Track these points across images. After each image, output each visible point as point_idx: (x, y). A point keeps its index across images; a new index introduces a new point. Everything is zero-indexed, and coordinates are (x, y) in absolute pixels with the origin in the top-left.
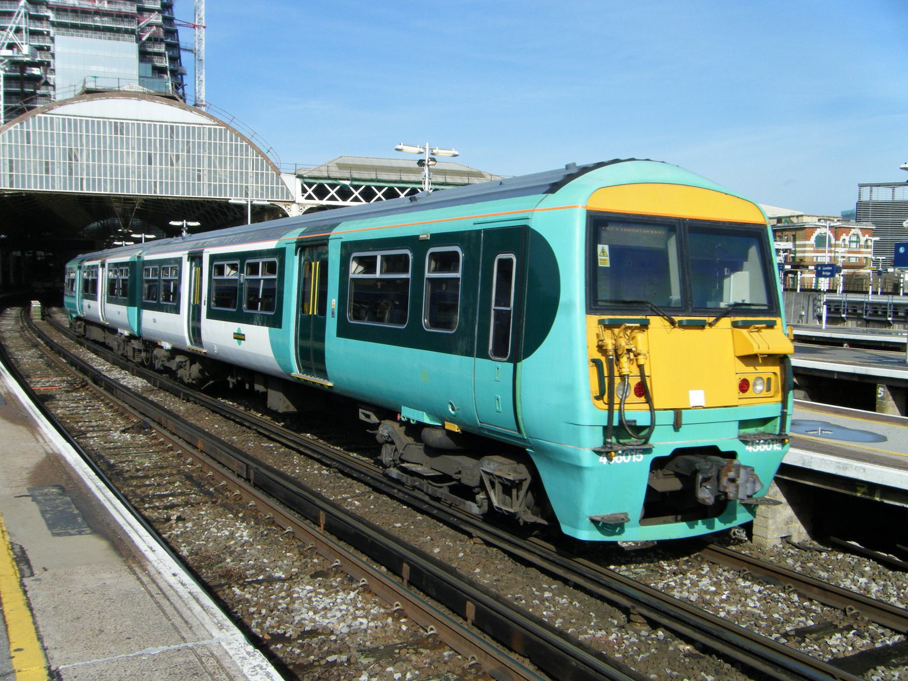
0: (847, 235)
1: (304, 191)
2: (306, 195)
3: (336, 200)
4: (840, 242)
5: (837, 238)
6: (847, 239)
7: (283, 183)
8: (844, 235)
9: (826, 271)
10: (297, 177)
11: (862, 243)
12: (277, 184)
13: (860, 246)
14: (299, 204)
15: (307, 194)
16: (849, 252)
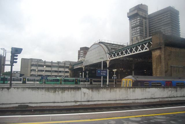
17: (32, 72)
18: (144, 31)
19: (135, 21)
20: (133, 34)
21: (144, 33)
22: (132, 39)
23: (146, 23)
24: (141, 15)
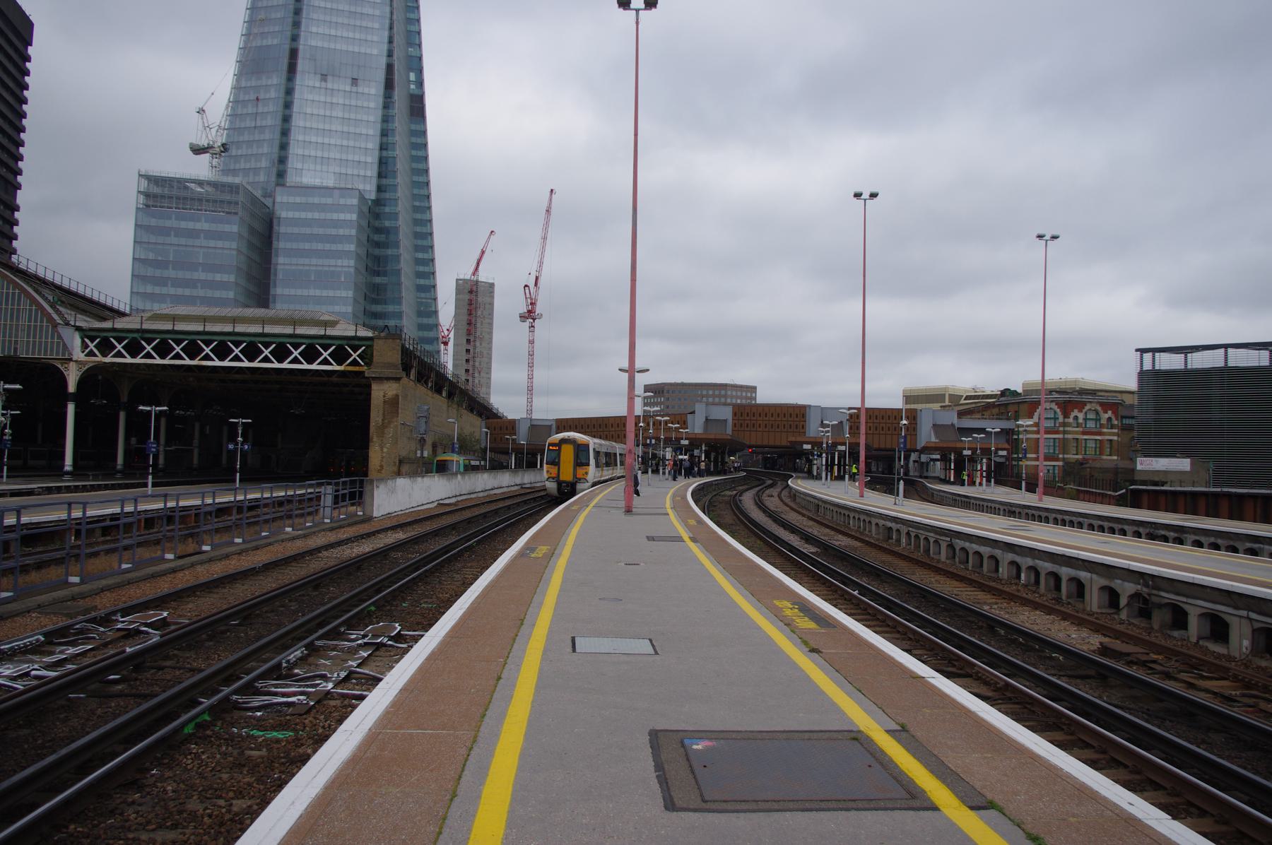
0: (1080, 411)
1: (85, 346)
2: (87, 351)
3: (124, 357)
4: (1071, 420)
5: (1066, 415)
6: (1081, 416)
7: (60, 337)
8: (1076, 411)
10: (76, 330)
11: (1104, 421)
12: (53, 338)
13: (1102, 426)
14: (76, 361)
15: (89, 349)
16: (1084, 433)
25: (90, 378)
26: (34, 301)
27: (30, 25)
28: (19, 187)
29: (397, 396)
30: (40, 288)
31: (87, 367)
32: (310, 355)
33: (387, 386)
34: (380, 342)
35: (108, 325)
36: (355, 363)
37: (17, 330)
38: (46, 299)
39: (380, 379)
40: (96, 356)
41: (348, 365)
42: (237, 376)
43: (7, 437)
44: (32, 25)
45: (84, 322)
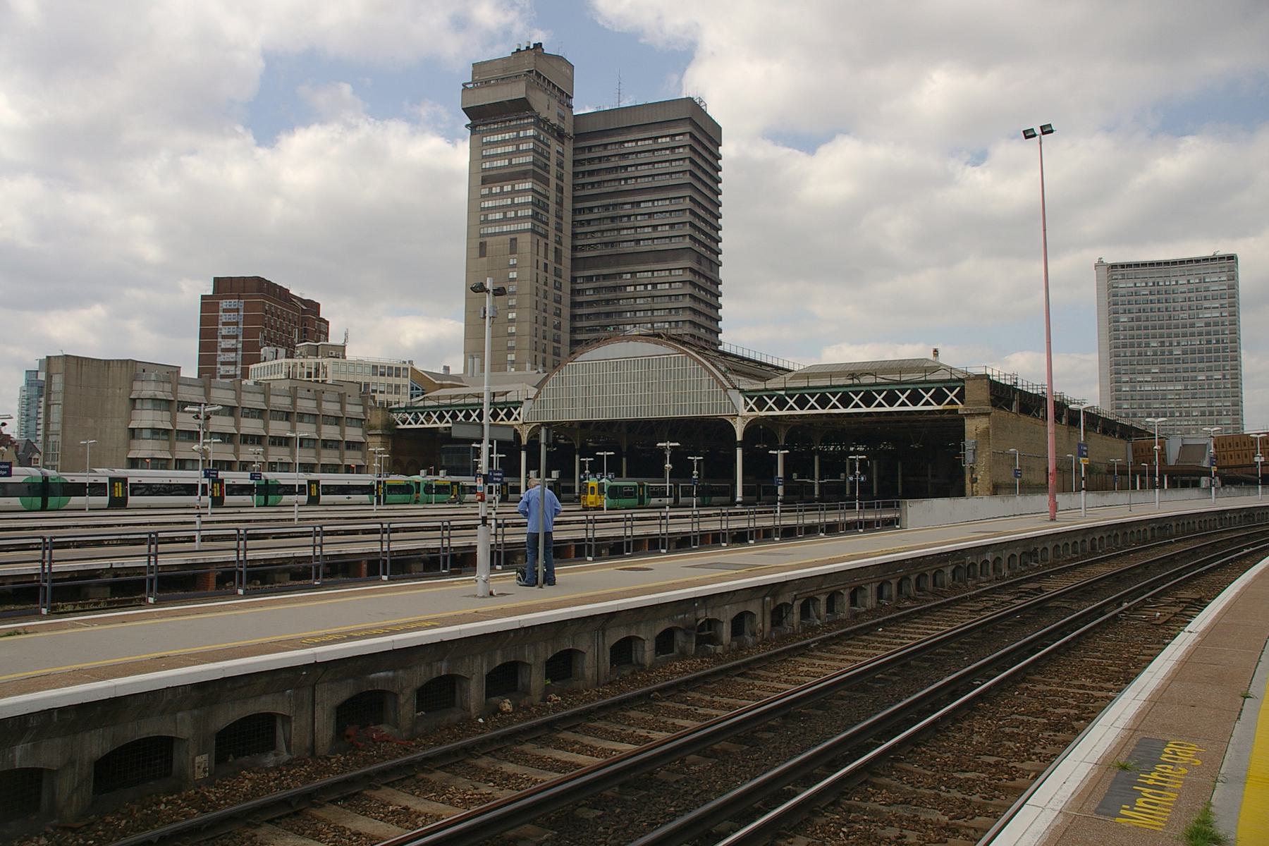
1: (746, 404)
2: (748, 407)
7: (730, 398)
9: (496, 477)
17: (135, 442)
18: (552, 207)
19: (504, 142)
20: (491, 217)
21: (552, 220)
22: (483, 246)
23: (560, 165)
24: (543, 116)
25: (753, 428)
26: (711, 373)
27: (718, 129)
28: (719, 264)
29: (987, 428)
30: (716, 362)
31: (749, 420)
32: (915, 398)
33: (978, 421)
34: (970, 382)
35: (761, 386)
36: (951, 402)
37: (701, 396)
38: (719, 370)
39: (971, 415)
40: (754, 411)
41: (947, 404)
42: (866, 418)
43: (694, 477)
44: (721, 128)
45: (746, 384)
